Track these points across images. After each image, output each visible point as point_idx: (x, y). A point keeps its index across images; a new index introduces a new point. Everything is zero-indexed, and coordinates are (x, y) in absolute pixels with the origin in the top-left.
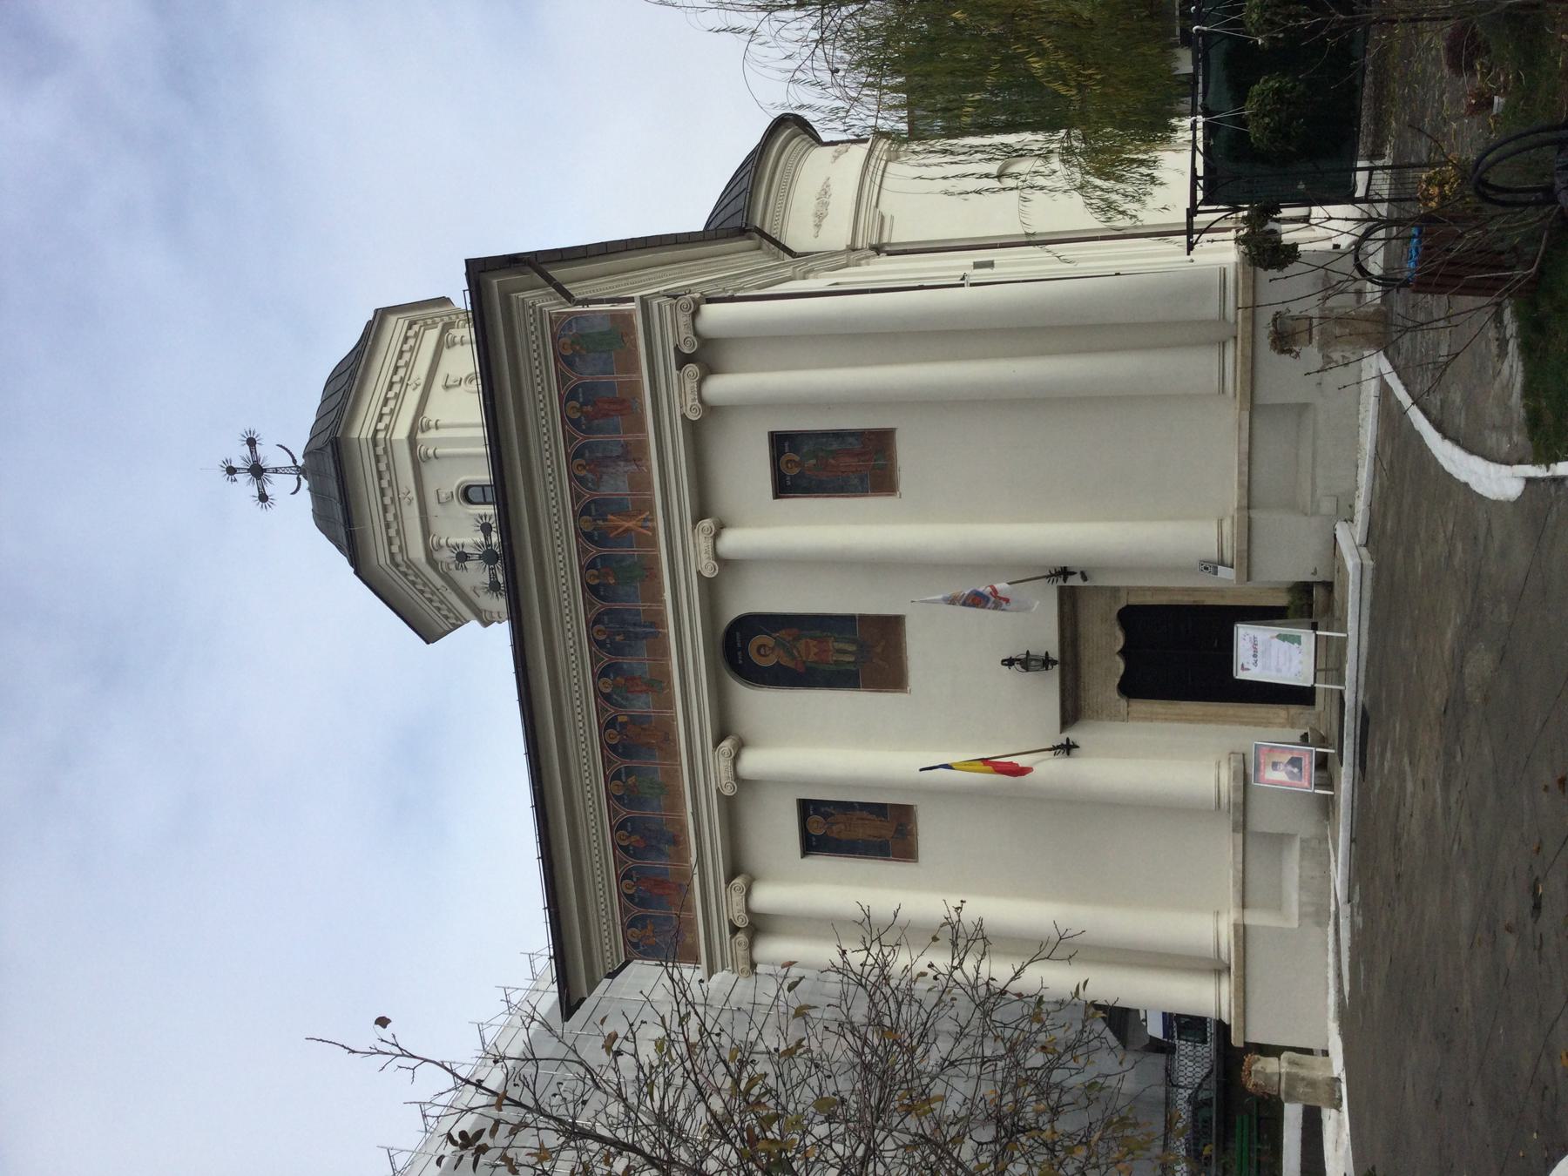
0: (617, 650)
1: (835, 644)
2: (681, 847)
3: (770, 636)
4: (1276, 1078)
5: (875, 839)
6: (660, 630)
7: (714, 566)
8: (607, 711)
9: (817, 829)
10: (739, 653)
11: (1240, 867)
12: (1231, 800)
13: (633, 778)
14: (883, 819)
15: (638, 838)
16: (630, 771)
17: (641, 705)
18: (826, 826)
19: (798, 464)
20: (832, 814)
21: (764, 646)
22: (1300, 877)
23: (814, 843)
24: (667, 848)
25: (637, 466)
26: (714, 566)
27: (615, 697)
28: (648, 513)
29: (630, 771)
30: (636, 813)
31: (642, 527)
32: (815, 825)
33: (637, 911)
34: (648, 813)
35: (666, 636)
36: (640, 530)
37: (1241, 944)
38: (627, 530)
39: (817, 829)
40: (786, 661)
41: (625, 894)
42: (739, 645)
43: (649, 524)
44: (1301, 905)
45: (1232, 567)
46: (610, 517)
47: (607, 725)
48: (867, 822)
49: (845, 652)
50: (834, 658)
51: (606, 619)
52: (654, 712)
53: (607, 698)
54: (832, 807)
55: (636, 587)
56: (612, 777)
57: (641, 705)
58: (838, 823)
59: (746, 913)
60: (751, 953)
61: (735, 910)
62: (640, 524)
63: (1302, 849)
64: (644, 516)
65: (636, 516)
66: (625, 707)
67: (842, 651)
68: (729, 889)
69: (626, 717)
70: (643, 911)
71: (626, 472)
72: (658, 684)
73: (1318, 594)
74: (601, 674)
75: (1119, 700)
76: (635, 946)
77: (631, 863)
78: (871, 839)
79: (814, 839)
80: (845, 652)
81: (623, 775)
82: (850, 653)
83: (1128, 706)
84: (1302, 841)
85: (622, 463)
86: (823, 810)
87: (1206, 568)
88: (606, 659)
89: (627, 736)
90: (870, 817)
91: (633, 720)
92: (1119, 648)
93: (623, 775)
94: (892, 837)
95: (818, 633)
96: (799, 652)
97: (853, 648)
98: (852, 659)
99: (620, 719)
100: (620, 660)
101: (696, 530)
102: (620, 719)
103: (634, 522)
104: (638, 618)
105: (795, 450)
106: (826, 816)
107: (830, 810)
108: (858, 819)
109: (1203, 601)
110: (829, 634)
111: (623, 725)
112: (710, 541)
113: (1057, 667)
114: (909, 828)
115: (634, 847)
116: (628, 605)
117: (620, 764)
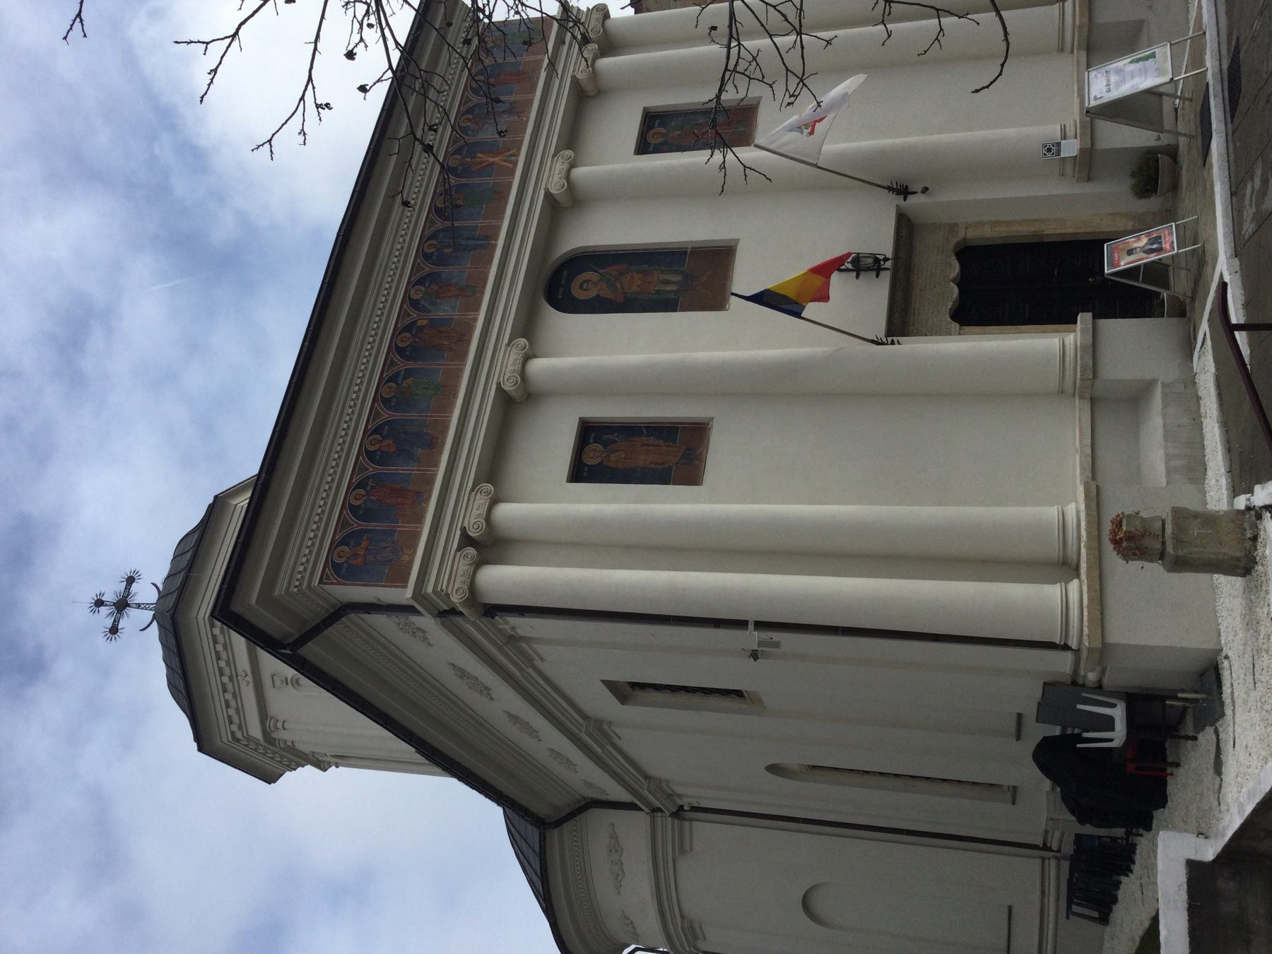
0: (442, 260)
1: (662, 275)
2: (434, 450)
3: (597, 272)
4: (1158, 524)
5: (658, 466)
6: (493, 242)
7: (564, 185)
8: (409, 315)
9: (594, 456)
10: (561, 289)
11: (1089, 451)
12: (1079, 344)
13: (410, 381)
14: (671, 444)
15: (391, 442)
16: (409, 373)
17: (445, 310)
18: (603, 455)
19: (662, 135)
20: (614, 441)
21: (587, 281)
22: (1164, 425)
23: (585, 474)
24: (419, 451)
25: (519, 116)
26: (564, 185)
27: (422, 302)
28: (515, 150)
29: (409, 373)
30: (397, 416)
31: (505, 161)
32: (592, 454)
33: (356, 525)
34: (413, 415)
35: (495, 246)
36: (505, 164)
37: (1094, 506)
38: (493, 164)
39: (592, 458)
40: (606, 293)
41: (350, 504)
42: (563, 282)
43: (514, 158)
44: (1168, 458)
45: (1076, 138)
46: (479, 155)
47: (405, 328)
48: (651, 448)
49: (667, 282)
50: (657, 288)
51: (441, 235)
52: (458, 315)
53: (415, 304)
54: (616, 434)
55: (482, 207)
56: (389, 376)
57: (445, 310)
58: (620, 450)
59: (485, 519)
60: (475, 573)
61: (473, 520)
62: (505, 159)
63: (1165, 395)
64: (511, 152)
65: (503, 153)
66: (430, 312)
67: (669, 281)
68: (473, 494)
69: (426, 321)
70: (364, 525)
71: (507, 122)
72: (471, 293)
73: (1164, 161)
74: (418, 280)
75: (950, 322)
76: (337, 568)
77: (372, 469)
78: (653, 466)
79: (586, 469)
80: (667, 282)
81: (401, 377)
82: (675, 283)
83: (960, 329)
84: (1164, 385)
85: (505, 116)
86: (605, 437)
87: (1049, 150)
88: (428, 268)
89: (420, 338)
90: (656, 442)
91: (433, 323)
92: (953, 275)
93: (401, 377)
94: (677, 463)
95: (646, 267)
96: (622, 285)
97: (678, 278)
98: (675, 289)
99: (419, 323)
100: (441, 269)
101: (556, 159)
102: (419, 323)
103: (500, 157)
104: (474, 233)
105: (663, 125)
106: (606, 444)
107: (614, 437)
108: (643, 445)
109: (1043, 231)
110: (657, 267)
111: (422, 327)
112: (566, 166)
113: (886, 277)
114: (698, 452)
115: (382, 451)
116: (466, 223)
117: (402, 365)
